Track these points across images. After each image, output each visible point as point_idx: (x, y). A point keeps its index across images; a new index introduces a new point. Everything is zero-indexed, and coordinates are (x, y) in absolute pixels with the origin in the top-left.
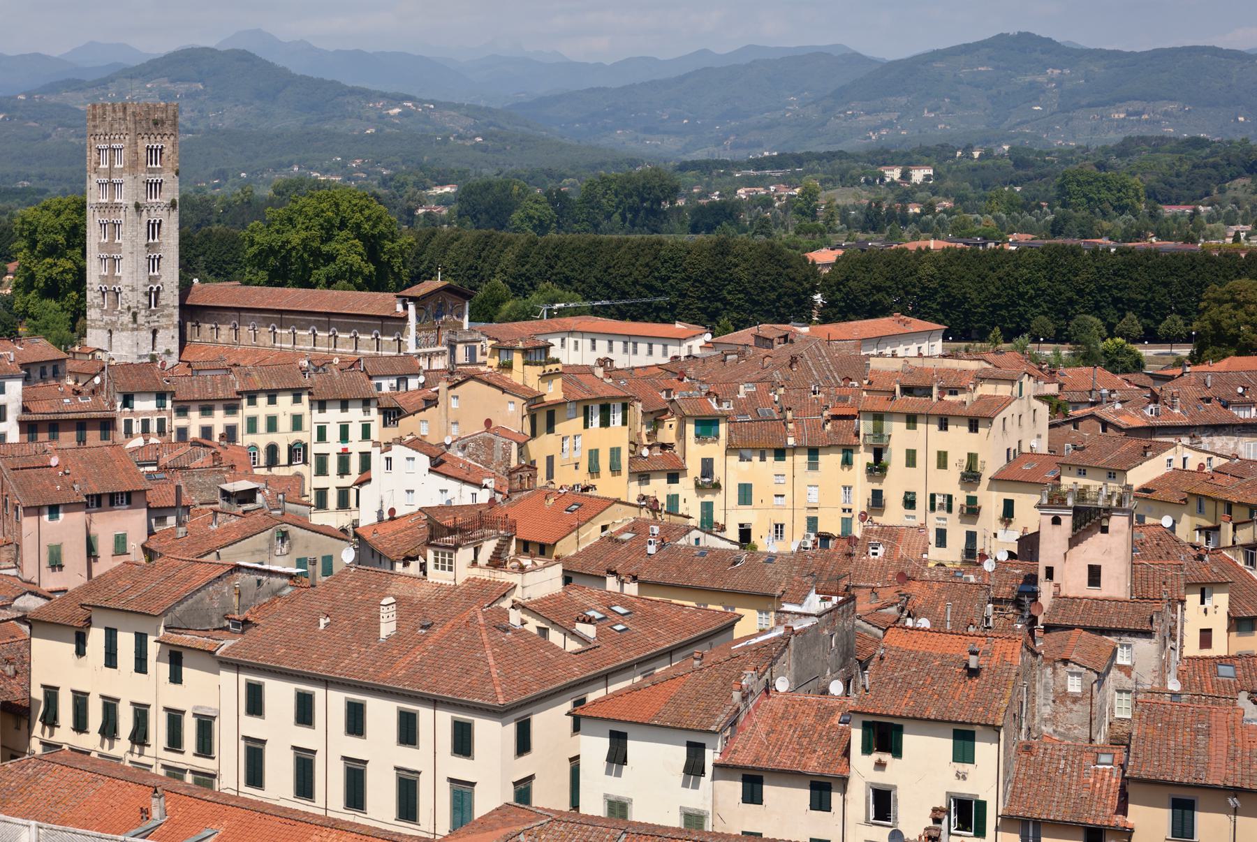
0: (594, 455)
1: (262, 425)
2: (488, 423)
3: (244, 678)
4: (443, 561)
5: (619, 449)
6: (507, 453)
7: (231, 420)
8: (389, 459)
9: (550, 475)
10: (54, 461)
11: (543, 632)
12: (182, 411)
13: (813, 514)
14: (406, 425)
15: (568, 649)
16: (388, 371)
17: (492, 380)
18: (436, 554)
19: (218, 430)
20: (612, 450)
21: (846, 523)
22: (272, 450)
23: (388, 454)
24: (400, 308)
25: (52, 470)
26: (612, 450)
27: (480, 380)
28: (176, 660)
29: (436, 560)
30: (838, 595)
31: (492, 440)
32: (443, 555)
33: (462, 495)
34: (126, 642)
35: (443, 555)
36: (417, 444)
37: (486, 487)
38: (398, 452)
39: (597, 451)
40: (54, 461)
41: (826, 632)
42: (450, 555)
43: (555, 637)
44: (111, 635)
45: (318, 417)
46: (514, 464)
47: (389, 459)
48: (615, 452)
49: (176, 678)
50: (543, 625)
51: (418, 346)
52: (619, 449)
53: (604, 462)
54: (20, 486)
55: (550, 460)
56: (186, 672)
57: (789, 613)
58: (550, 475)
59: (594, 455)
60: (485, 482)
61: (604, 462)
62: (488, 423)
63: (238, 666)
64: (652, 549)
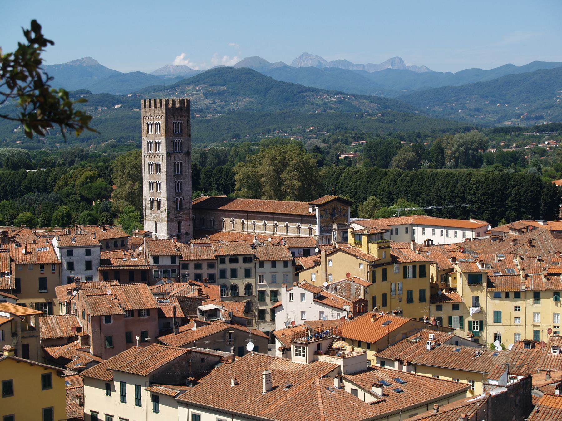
0: (410, 294)
1: (228, 273)
2: (348, 275)
3: (191, 411)
4: (300, 351)
5: (424, 291)
6: (358, 291)
7: (211, 271)
8: (291, 295)
9: (384, 304)
10: (109, 292)
11: (354, 391)
12: (185, 267)
13: (536, 329)
14: (303, 275)
15: (366, 402)
16: (298, 245)
17: (351, 251)
18: (296, 347)
19: (205, 277)
20: (420, 291)
21: (536, 333)
22: (235, 288)
23: (290, 292)
24: (311, 210)
25: (107, 297)
26: (420, 291)
27: (344, 252)
28: (156, 399)
29: (296, 351)
30: (521, 375)
31: (350, 285)
32: (300, 348)
33: (330, 315)
34: (130, 389)
35: (300, 348)
36: (307, 286)
37: (345, 310)
38: (296, 291)
39: (412, 291)
40: (109, 292)
41: (512, 396)
42: (304, 348)
43: (361, 394)
44: (123, 385)
45: (259, 271)
46: (362, 297)
47: (291, 295)
48: (422, 293)
49: (156, 410)
50: (355, 387)
51: (321, 231)
52: (424, 291)
53: (416, 296)
54: (90, 305)
55: (384, 296)
56: (161, 407)
57: (491, 385)
58: (384, 304)
59: (410, 294)
60: (344, 308)
61: (416, 296)
62: (348, 275)
63: (188, 405)
64: (428, 347)
